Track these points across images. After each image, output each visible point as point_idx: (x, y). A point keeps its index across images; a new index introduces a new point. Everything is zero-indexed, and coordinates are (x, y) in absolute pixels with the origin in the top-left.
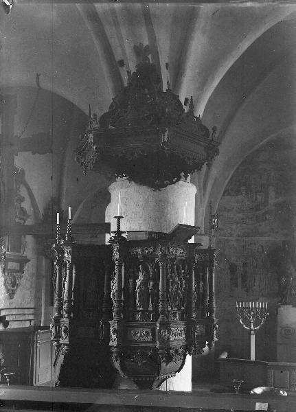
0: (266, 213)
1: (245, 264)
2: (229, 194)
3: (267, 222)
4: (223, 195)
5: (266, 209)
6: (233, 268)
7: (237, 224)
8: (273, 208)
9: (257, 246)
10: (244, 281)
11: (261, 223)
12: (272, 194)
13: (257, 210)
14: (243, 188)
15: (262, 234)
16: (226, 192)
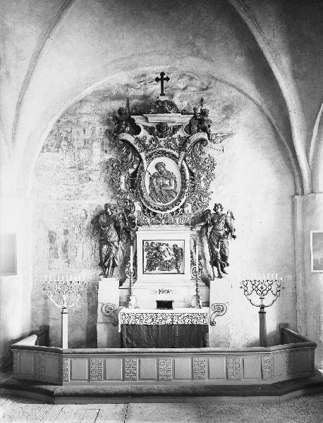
0: (91, 172)
1: (66, 232)
2: (49, 151)
3: (91, 182)
4: (42, 151)
5: (90, 168)
6: (52, 238)
7: (58, 184)
8: (98, 167)
9: (80, 210)
10: (65, 250)
11: (83, 184)
12: (97, 149)
13: (80, 169)
14: (64, 143)
15: (86, 197)
16: (46, 148)
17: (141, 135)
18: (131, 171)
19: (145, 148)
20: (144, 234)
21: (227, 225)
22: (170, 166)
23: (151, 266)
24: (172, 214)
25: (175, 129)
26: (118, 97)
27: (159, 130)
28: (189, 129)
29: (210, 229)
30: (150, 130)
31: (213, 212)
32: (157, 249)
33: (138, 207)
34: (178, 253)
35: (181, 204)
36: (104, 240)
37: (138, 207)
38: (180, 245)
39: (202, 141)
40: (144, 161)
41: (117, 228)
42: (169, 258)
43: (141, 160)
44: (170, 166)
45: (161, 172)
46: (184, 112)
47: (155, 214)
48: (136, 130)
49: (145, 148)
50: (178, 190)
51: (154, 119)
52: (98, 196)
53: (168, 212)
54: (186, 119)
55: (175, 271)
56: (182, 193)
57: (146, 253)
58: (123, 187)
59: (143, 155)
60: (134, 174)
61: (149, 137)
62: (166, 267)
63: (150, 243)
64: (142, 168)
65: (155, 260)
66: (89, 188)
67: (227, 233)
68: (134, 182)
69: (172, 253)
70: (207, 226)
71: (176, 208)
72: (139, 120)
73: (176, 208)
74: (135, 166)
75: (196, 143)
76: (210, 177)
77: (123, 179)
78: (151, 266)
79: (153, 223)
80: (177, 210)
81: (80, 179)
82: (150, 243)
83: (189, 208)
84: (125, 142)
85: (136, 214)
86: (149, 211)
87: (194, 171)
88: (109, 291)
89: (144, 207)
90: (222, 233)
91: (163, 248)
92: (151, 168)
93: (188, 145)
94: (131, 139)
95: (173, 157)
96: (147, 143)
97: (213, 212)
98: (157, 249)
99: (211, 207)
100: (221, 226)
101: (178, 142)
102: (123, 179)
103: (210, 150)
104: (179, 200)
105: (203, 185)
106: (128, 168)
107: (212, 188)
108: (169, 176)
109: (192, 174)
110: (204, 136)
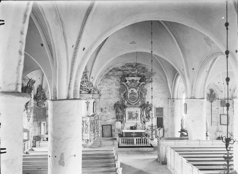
17: (127, 82)
18: (124, 92)
19: (128, 86)
20: (127, 110)
21: (150, 107)
22: (135, 91)
23: (130, 118)
24: (135, 104)
25: (137, 81)
26: (120, 70)
27: (132, 81)
28: (140, 81)
29: (146, 108)
30: (130, 81)
31: (146, 104)
32: (131, 113)
33: (126, 102)
34: (137, 114)
35: (138, 102)
36: (117, 112)
37: (126, 102)
38: (137, 112)
39: (144, 84)
40: (128, 90)
41: (121, 108)
42: (134, 116)
43: (127, 89)
44: (135, 91)
45: (132, 93)
46: (139, 76)
47: (131, 104)
48: (126, 81)
49: (128, 86)
50: (137, 97)
51: (131, 78)
52: (115, 99)
53: (135, 103)
54: (139, 78)
55: (136, 119)
56: (138, 98)
57: (128, 115)
58: (122, 96)
59: (128, 88)
60: (125, 93)
61: (129, 83)
62: (134, 118)
63: (129, 112)
64: (127, 91)
65: (131, 117)
66: (111, 96)
67: (150, 110)
68: (125, 95)
69: (135, 114)
70: (145, 107)
71: (136, 103)
72: (126, 78)
73: (136, 103)
74: (126, 91)
75: (142, 85)
76: (146, 94)
77: (122, 94)
78: (130, 118)
79: (131, 107)
80: (137, 103)
81: (109, 93)
82: (129, 112)
83: (140, 103)
84: (123, 84)
85: (125, 104)
86: (129, 103)
87: (141, 92)
88: (119, 125)
89: (128, 102)
90: (149, 109)
91: (133, 113)
92: (130, 92)
93: (140, 85)
94: (124, 83)
95: (136, 89)
96: (129, 84)
97: (146, 104)
98: (131, 113)
99: (146, 102)
100: (149, 108)
101: (137, 84)
102: (122, 94)
103: (145, 87)
104: (137, 101)
105: (144, 96)
106: (123, 92)
107: (146, 97)
108: (135, 94)
109: (141, 93)
110: (144, 83)
